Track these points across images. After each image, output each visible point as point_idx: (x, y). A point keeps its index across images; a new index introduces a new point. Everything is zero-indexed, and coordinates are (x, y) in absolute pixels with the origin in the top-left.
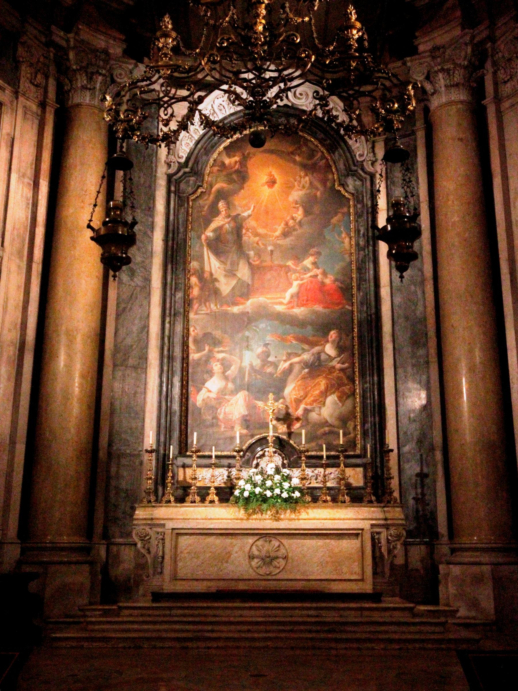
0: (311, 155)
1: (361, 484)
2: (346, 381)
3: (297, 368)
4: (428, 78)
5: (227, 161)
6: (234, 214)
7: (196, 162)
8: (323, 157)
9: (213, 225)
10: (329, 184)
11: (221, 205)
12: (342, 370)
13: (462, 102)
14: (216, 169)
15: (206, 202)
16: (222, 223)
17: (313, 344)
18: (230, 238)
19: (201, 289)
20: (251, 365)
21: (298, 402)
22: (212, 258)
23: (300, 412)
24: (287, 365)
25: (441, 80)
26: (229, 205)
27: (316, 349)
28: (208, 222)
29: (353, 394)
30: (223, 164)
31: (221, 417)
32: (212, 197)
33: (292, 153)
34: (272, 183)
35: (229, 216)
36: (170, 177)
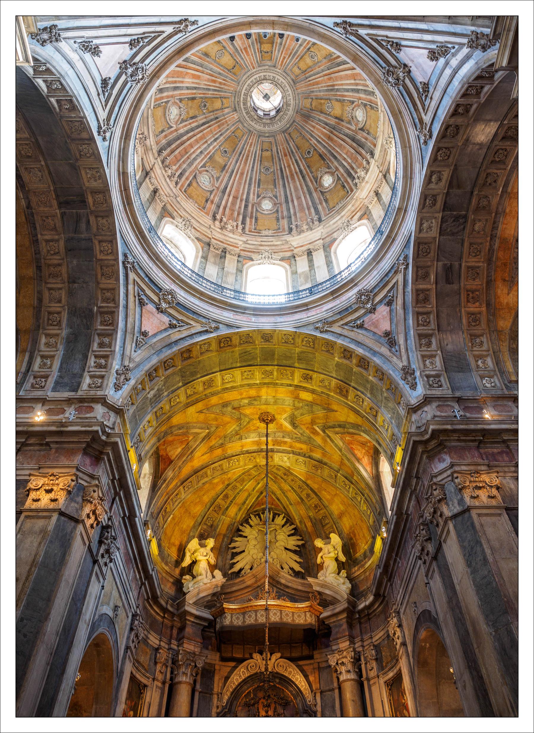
7: (231, 705)
25: (343, 669)
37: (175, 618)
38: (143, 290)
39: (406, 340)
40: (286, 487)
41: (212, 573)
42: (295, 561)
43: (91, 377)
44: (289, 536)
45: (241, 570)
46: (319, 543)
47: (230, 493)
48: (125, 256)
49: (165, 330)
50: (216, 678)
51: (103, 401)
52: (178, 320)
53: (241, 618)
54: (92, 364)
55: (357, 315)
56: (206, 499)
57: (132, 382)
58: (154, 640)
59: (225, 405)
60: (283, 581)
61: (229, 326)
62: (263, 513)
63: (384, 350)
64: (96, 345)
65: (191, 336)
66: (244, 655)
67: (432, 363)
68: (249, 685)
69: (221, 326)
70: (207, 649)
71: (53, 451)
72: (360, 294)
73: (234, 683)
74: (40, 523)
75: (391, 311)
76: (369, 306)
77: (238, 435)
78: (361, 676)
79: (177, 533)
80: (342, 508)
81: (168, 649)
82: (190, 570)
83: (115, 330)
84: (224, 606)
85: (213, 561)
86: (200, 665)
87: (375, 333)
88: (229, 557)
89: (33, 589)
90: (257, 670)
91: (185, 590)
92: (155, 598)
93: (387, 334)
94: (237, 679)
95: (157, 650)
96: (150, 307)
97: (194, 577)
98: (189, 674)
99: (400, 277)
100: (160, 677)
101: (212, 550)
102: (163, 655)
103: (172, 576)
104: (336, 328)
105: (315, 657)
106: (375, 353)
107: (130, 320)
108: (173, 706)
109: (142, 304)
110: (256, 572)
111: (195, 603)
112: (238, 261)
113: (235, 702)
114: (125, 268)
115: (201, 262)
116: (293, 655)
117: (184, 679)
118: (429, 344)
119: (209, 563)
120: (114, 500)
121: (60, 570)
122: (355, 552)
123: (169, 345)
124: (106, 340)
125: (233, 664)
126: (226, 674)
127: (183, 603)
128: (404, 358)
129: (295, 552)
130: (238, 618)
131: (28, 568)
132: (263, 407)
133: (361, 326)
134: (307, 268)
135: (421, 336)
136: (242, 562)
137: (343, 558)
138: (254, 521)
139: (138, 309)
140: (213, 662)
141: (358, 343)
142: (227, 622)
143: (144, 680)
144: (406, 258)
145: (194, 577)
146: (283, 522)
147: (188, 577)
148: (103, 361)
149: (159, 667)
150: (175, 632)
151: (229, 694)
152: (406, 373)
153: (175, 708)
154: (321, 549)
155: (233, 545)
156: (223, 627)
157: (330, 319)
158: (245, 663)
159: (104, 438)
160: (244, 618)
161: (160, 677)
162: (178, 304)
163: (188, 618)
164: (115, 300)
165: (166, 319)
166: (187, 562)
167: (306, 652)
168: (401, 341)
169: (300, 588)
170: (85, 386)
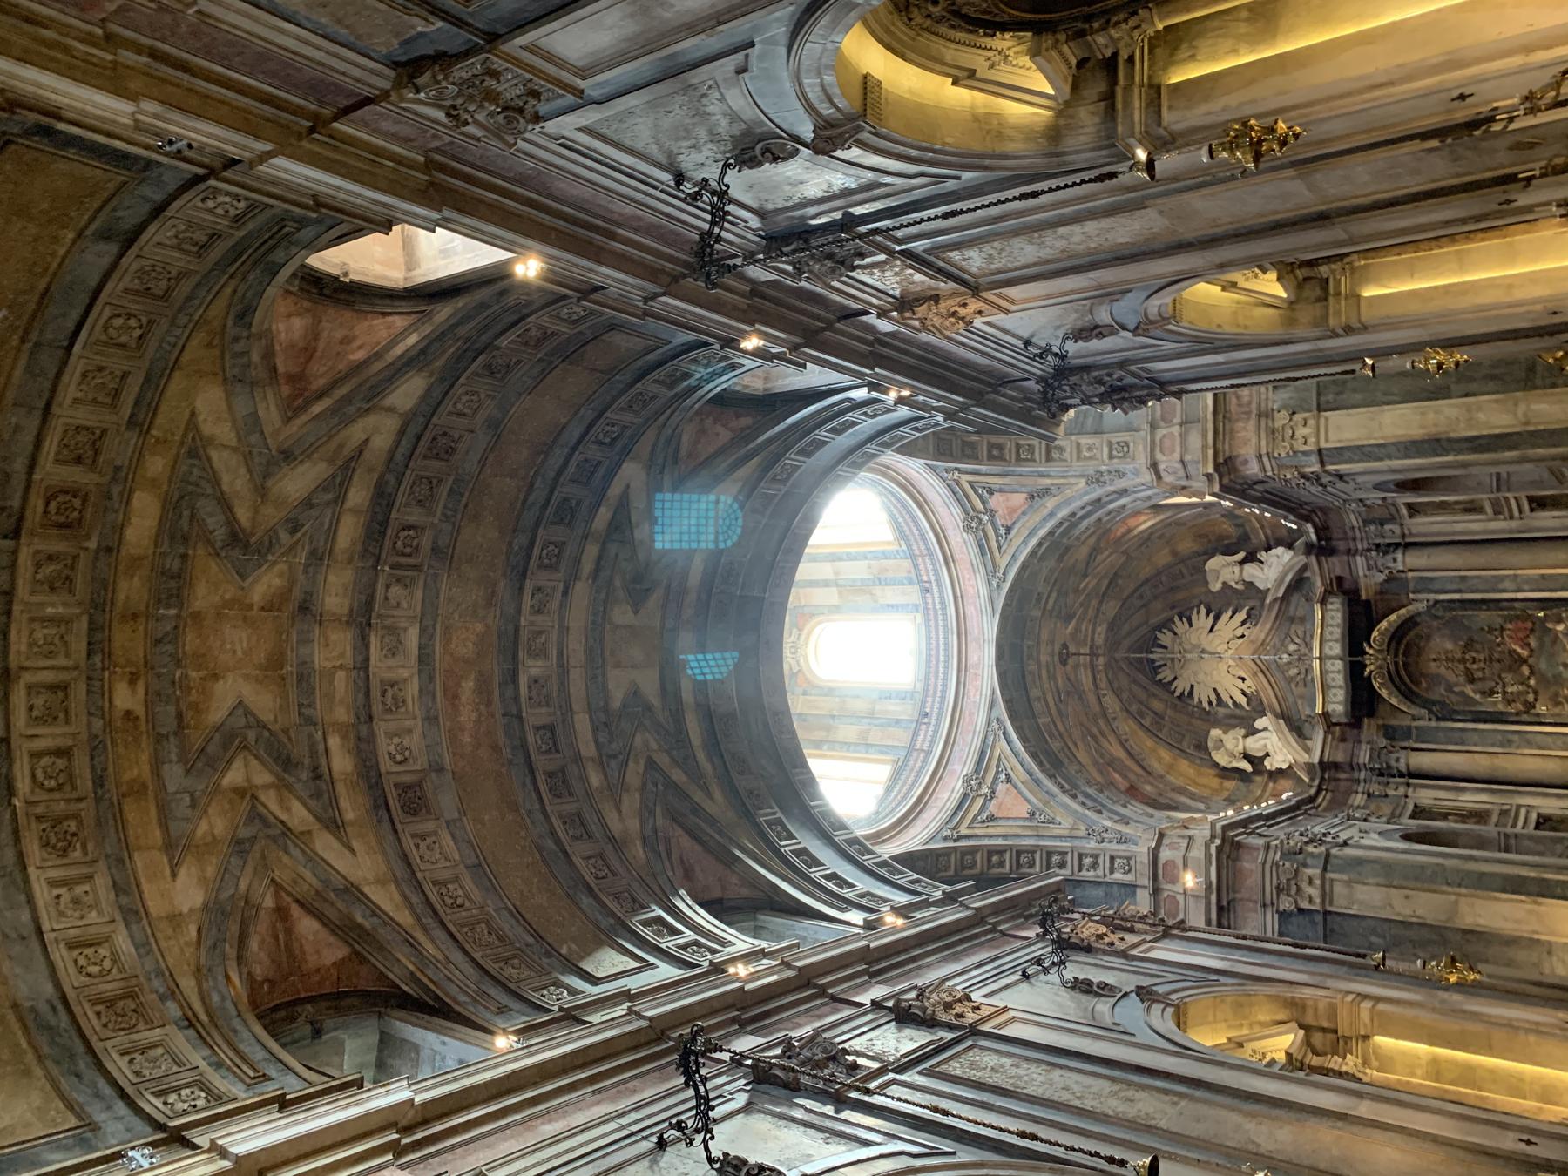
0: (1419, 637)
9: (1471, 694)
15: (1454, 698)
17: (1557, 637)
36: (1438, 719)
38: (975, 817)
39: (1048, 476)
40: (1126, 628)
41: (1258, 731)
43: (1112, 871)
44: (1191, 625)
45: (1244, 693)
46: (1216, 586)
47: (1134, 708)
48: (946, 839)
49: (1016, 787)
50: (1394, 722)
51: (1155, 853)
52: (998, 773)
54: (1092, 873)
55: (991, 534)
56: (1149, 743)
57: (1108, 823)
58: (1359, 799)
59: (1059, 711)
60: (1262, 636)
61: (992, 704)
62: (1153, 661)
63: (1050, 503)
64: (1063, 872)
65: (1016, 754)
67: (1090, 449)
69: (994, 715)
71: (1238, 896)
72: (968, 528)
74: (1339, 889)
75: (1001, 491)
76: (985, 518)
77: (1081, 696)
78: (1397, 545)
79: (1203, 780)
80: (1166, 551)
82: (1256, 761)
83: (1041, 848)
85: (1243, 732)
86: (1383, 742)
87: (1024, 513)
88: (1221, 711)
89: (1416, 879)
91: (1284, 766)
92: (1312, 799)
93: (1032, 497)
95: (1369, 795)
96: (992, 807)
97: (1267, 755)
99: (965, 479)
100: (1402, 790)
101: (1225, 733)
102: (1376, 789)
103: (1266, 785)
104: (1003, 562)
106: (1051, 515)
107: (1019, 831)
109: (992, 818)
111: (1308, 750)
112: (805, 694)
114: (960, 838)
115: (829, 749)
118: (1061, 449)
119: (1245, 736)
120: (1260, 835)
122: (1228, 537)
123: (1037, 782)
124: (1055, 859)
127: (1309, 768)
128: (1073, 481)
129: (1217, 618)
131: (1393, 891)
132: (1056, 658)
133: (1008, 529)
134: (834, 589)
135: (1049, 458)
136: (1233, 690)
137: (1241, 555)
138: (1166, 675)
139: (1001, 823)
141: (1031, 534)
142: (1340, 708)
143: (1411, 807)
144: (947, 470)
146: (1169, 634)
147: (1267, 763)
148: (1087, 861)
149: (1391, 792)
150: (1343, 776)
152: (1098, 481)
154: (1224, 583)
155: (1205, 705)
156: (1346, 713)
157: (990, 567)
159: (1218, 842)
161: (1402, 790)
162: (977, 769)
164: (1000, 851)
165: (1002, 788)
166: (1248, 767)
168: (1048, 481)
170: (1128, 878)
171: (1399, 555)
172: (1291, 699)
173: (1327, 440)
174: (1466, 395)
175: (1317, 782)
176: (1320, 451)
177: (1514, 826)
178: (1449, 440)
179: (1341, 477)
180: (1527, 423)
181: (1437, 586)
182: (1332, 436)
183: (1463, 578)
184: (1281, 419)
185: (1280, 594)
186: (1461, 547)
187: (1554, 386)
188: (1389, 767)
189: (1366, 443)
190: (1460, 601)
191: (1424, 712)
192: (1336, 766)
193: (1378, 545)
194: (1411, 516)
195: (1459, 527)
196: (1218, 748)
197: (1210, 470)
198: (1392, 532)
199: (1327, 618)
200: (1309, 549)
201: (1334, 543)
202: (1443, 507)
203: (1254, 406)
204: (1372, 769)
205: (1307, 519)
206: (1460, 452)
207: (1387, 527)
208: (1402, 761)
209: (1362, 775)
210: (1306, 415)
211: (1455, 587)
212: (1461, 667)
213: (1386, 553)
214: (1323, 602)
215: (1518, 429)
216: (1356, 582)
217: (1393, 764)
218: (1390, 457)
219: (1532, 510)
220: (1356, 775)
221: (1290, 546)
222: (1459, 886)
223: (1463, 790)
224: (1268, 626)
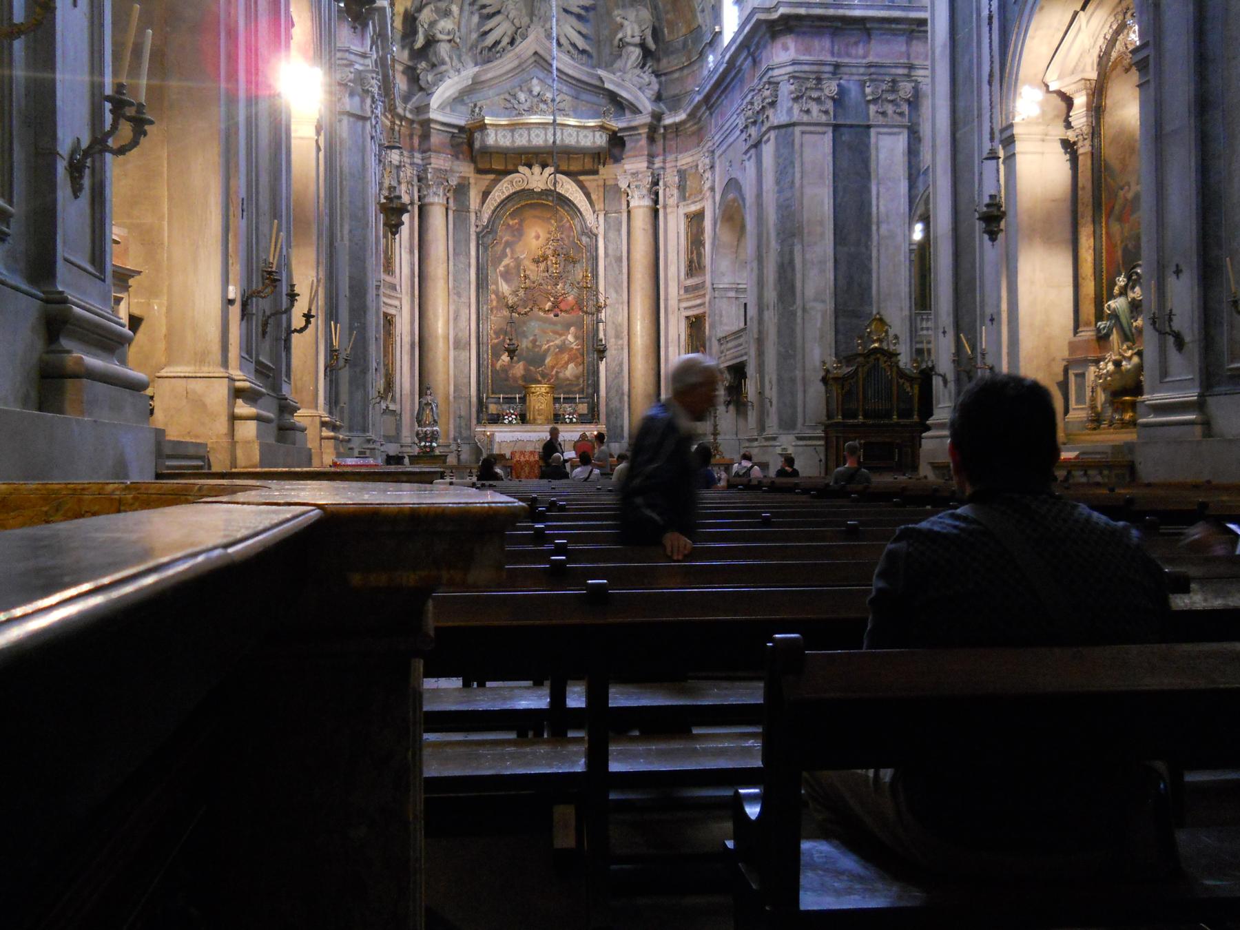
1: (586, 412)
2: (579, 355)
3: (552, 349)
4: (629, 186)
5: (511, 223)
6: (516, 256)
7: (493, 225)
8: (568, 221)
9: (503, 263)
10: (571, 239)
11: (508, 250)
12: (576, 349)
13: (644, 207)
14: (504, 227)
15: (499, 248)
16: (508, 262)
17: (561, 335)
18: (514, 271)
19: (498, 302)
20: (527, 348)
21: (553, 367)
22: (504, 283)
23: (554, 373)
24: (546, 347)
26: (513, 252)
27: (564, 337)
28: (500, 261)
29: (583, 363)
30: (509, 224)
31: (510, 375)
32: (502, 245)
33: (550, 218)
34: (538, 237)
35: (512, 258)
36: (478, 234)
37: (415, 126)
42: (580, 33)
45: (497, 43)
53: (509, 135)
66: (506, 166)
68: (513, 203)
70: (458, 158)
73: (495, 200)
78: (656, 202)
81: (411, 164)
82: (424, 53)
84: (486, 122)
86: (454, 182)
88: (476, 19)
90: (524, 186)
94: (499, 196)
95: (398, 167)
98: (441, 195)
105: (600, 173)
108: (427, 229)
110: (521, 50)
111: (441, 107)
113: (497, 221)
116: (574, 168)
117: (436, 200)
121: (364, 177)
125: (492, 176)
126: (483, 189)
129: (579, 17)
130: (504, 136)
137: (651, 44)
140: (467, 175)
145: (434, 66)
147: (424, 64)
150: (416, 141)
151: (490, 212)
153: (430, 231)
158: (509, 177)
160: (513, 136)
163: (432, 125)
166: (420, 41)
167: (588, 165)
169: (585, 78)
171: (647, 202)
172: (491, 93)
173: (803, 133)
174: (836, 261)
175: (409, 116)
176: (794, 125)
177: (385, 295)
178: (792, 245)
179: (757, 145)
180: (804, 310)
181: (612, 235)
182: (806, 137)
183: (620, 260)
184: (831, 88)
185: (607, 85)
186: (651, 256)
187: (837, 332)
188: (428, 186)
189: (797, 169)
190: (596, 259)
191: (485, 221)
192: (425, 136)
193: (657, 183)
194: (687, 216)
195: (672, 256)
196: (437, 10)
197: (782, 10)
198: (669, 195)
199: (586, 132)
200: (657, 117)
201: (660, 143)
202: (696, 242)
203: (846, 60)
204: (425, 170)
205: (692, 115)
206: (781, 254)
207: (675, 192)
208: (436, 200)
209: (420, 162)
210: (832, 113)
211: (610, 252)
212: (549, 252)
213: (650, 190)
214: (602, 128)
215: (799, 302)
216: (617, 160)
217: (431, 191)
218: (780, 191)
219: (687, 317)
220: (417, 155)
221: (658, 98)
222: (350, 240)
223: (411, 252)
224: (570, 72)
